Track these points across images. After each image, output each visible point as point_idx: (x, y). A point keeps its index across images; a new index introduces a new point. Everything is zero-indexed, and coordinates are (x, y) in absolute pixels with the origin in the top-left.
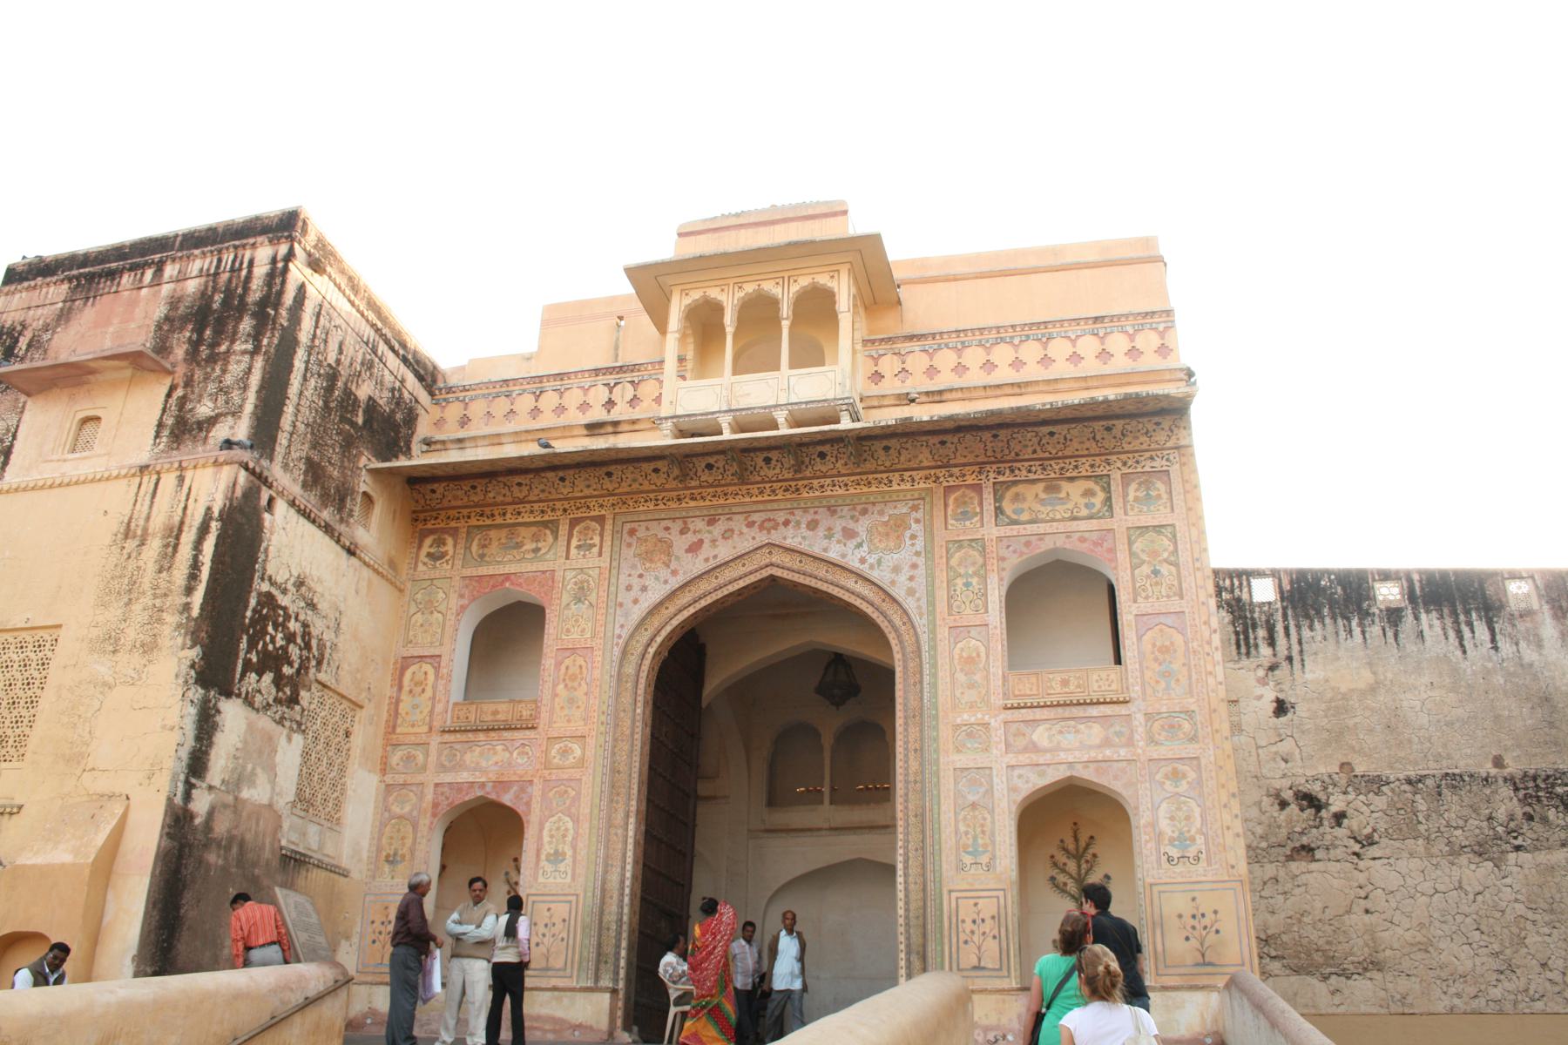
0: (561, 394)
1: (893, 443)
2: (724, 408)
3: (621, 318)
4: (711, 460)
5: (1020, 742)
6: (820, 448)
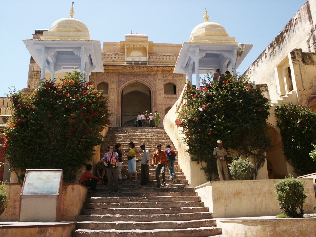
0: (108, 56)
1: (152, 67)
2: (133, 61)
3: (115, 45)
4: (130, 67)
5: (165, 102)
6: (143, 67)
